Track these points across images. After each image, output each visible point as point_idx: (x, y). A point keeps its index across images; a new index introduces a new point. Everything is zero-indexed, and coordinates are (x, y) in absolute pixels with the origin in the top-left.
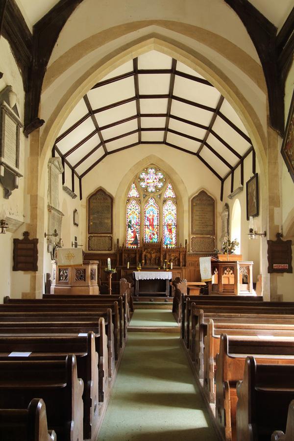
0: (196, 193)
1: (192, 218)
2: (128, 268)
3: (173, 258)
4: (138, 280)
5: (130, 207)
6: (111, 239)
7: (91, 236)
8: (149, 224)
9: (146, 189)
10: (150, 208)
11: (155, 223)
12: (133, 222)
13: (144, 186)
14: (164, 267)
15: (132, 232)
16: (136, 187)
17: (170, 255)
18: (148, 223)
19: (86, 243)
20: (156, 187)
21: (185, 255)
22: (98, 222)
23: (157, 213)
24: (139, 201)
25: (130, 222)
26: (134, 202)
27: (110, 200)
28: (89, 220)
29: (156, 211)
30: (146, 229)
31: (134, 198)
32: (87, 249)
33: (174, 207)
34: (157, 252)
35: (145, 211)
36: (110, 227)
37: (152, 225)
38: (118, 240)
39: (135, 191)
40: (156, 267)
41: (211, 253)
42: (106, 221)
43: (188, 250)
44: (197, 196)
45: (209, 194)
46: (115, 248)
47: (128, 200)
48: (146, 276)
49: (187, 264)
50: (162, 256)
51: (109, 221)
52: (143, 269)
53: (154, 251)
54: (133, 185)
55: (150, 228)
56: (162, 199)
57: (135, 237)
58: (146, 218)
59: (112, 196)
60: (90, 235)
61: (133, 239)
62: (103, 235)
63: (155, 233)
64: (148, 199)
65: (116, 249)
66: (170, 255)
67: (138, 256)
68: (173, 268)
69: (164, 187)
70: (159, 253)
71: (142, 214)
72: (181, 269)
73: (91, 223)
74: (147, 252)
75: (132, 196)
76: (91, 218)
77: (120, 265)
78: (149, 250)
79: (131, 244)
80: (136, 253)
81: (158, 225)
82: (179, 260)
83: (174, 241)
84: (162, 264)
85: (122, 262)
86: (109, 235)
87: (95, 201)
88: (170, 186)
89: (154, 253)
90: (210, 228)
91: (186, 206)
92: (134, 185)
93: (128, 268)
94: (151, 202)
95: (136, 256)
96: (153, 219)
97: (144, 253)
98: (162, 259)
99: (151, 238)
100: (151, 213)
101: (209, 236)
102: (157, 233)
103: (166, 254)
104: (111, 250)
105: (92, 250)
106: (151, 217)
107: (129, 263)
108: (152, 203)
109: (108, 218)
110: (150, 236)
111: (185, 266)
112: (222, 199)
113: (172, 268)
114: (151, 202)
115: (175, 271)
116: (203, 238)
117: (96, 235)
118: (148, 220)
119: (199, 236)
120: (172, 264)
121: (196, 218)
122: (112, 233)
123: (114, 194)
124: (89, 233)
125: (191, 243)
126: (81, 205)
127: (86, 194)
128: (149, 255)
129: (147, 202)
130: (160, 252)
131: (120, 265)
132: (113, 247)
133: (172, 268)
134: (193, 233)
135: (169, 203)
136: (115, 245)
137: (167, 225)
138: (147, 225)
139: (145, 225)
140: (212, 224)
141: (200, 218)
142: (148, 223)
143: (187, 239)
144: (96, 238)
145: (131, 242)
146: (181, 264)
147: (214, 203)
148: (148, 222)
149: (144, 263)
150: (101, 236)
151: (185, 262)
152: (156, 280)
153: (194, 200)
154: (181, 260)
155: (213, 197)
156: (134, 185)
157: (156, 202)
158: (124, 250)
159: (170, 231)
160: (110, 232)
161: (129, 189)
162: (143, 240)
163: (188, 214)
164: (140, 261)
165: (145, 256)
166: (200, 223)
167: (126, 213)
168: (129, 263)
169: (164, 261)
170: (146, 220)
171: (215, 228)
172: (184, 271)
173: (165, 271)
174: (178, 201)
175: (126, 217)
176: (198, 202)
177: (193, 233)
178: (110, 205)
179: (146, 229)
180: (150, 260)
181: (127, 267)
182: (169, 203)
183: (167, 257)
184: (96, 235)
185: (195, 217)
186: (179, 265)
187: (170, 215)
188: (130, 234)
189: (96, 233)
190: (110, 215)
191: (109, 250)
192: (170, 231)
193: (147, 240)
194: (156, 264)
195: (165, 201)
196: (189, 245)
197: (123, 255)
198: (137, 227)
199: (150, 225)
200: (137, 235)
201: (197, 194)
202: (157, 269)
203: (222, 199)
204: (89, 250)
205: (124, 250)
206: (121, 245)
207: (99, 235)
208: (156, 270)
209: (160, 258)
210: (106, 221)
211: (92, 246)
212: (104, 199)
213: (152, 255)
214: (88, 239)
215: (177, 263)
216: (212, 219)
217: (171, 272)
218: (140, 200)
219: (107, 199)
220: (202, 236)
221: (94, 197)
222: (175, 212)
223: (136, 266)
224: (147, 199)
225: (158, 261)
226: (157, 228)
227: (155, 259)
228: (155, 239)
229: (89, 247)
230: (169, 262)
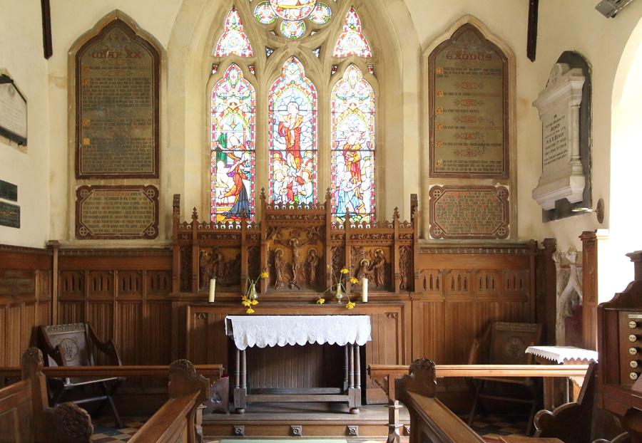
0: (447, 30)
1: (432, 118)
2: (212, 299)
3: (367, 261)
4: (242, 348)
5: (221, 90)
6: (155, 195)
7: (85, 187)
8: (283, 147)
9: (274, 30)
10: (288, 92)
11: (306, 144)
12: (233, 141)
13: (266, 21)
14: (340, 295)
15: (230, 174)
16: (241, 22)
17: (357, 251)
18: (280, 144)
19: (68, 212)
20: (307, 22)
21: (410, 252)
22: (108, 136)
23: (310, 108)
24: (251, 68)
25: (224, 140)
26: (234, 73)
27: (148, 59)
28: (78, 130)
29: (307, 102)
30: (277, 165)
31: (236, 62)
32: (73, 233)
33: (367, 90)
34: (312, 242)
35: (272, 104)
36: (152, 159)
37: (294, 150)
38: (177, 199)
39: (239, 36)
40: (309, 294)
41: (497, 241)
42: (137, 133)
43: (419, 234)
44: (447, 43)
45: (489, 37)
46: (167, 229)
47: (216, 66)
48: (274, 336)
49: (418, 284)
50: (330, 255)
51: (149, 134)
52: (269, 306)
53: (303, 236)
54: (233, 17)
55: (290, 158)
56: (328, 61)
57: (241, 192)
58: (276, 128)
59: (155, 41)
60: (82, 183)
61: (232, 199)
62: (126, 182)
63: (305, 176)
64: (281, 62)
65: (171, 233)
66: (357, 251)
67: (246, 255)
68: (369, 298)
69: (335, 21)
70: (320, 244)
71: (261, 110)
72: (397, 300)
73: (86, 142)
74: (277, 242)
75: (227, 52)
76: (86, 121)
77: (183, 289)
78: (286, 233)
79: (227, 215)
80: (239, 247)
81: (314, 151)
82: (389, 267)
83: (367, 206)
84: (330, 283)
85: (190, 279)
86: (147, 183)
87: (97, 62)
88: (352, 19)
89: (300, 246)
90: (491, 155)
91: (411, 78)
92: (235, 14)
93: (212, 299)
94: (293, 71)
95: (239, 257)
96: (298, 130)
97: (268, 245)
98: (329, 267)
99: (291, 195)
100: (293, 110)
101: (488, 182)
102: (311, 177)
103: (343, 247)
104: (154, 237)
105: (89, 236)
106: (289, 124)
107: (213, 282)
108: (296, 77)
109: (142, 123)
110: (289, 188)
111: (410, 288)
112: (531, 54)
113: (365, 299)
114: (293, 71)
115: (375, 310)
116: (470, 188)
117: (102, 182)
118: (280, 133)
119: (455, 182)
120: (365, 281)
121: (446, 118)
122: (157, 175)
123: (163, 39)
124: (78, 177)
125: (427, 206)
126: (51, 77)
127: (64, 38)
128: (284, 253)
129: (277, 71)
130: (324, 240)
131: (183, 289)
132: (162, 226)
133: (365, 299)
134: (434, 173)
135: (352, 75)
136: (167, 217)
137: (345, 151)
138: (279, 152)
139: (273, 151)
140: (500, 141)
141: (457, 119)
142: (280, 144)
143: (416, 191)
144: (103, 195)
145: (227, 209)
146: (398, 283)
147: (505, 65)
148: (283, 140)
149: (267, 283)
150: (120, 188)
151: (411, 275)
152: (311, 348)
153: (439, 57)
154: (397, 270)
155: (501, 46)
156: (235, 14)
157: (309, 75)
158: (199, 235)
159: (356, 169)
160: (151, 170)
161: (218, 26)
162: (263, 197)
163: (416, 106)
164: (255, 273)
165: (273, 255)
166: (457, 136)
167: (206, 111)
168: (213, 282)
169: (338, 275)
170: (276, 134)
171: (511, 155)
172: (408, 305)
173: (343, 310)
174: (380, 68)
175: (206, 126)
176: (452, 64)
177: (434, 173)
178: (149, 74)
179: (277, 165)
180: (290, 269)
181: (208, 297)
182: (352, 75)
183: (349, 256)
184: (102, 182)
185: (443, 118)
186: (389, 286)
187: (354, 117)
188: (223, 182)
189: (104, 177)
190: (151, 111)
191: (147, 237)
192: (356, 169)
193: (278, 193)
194: (309, 284)
195: (336, 68)
196: (422, 212)
197: (196, 251)
198: (247, 156)
199: (288, 150)
200: (247, 184)
201: (447, 36)
202: (314, 301)
203: (531, 54)
204: (78, 236)
205: (199, 235)
206: (187, 217)
207: (113, 183)
208: (307, 307)
209: (322, 262)
210: (137, 133)
211: (89, 222)
212: (129, 54)
213: (297, 252)
214: (74, 199)
215: (381, 281)
216: (498, 123)
217: (367, 318)
218: (253, 67)
219: (138, 55)
220: (465, 182)
221: (95, 47)
222: (369, 104)
223: (241, 292)
224: (277, 60)
225: (317, 275)
226: (312, 160)
227: (308, 265)
228: (307, 195)
229: (78, 225)
230: (356, 276)
